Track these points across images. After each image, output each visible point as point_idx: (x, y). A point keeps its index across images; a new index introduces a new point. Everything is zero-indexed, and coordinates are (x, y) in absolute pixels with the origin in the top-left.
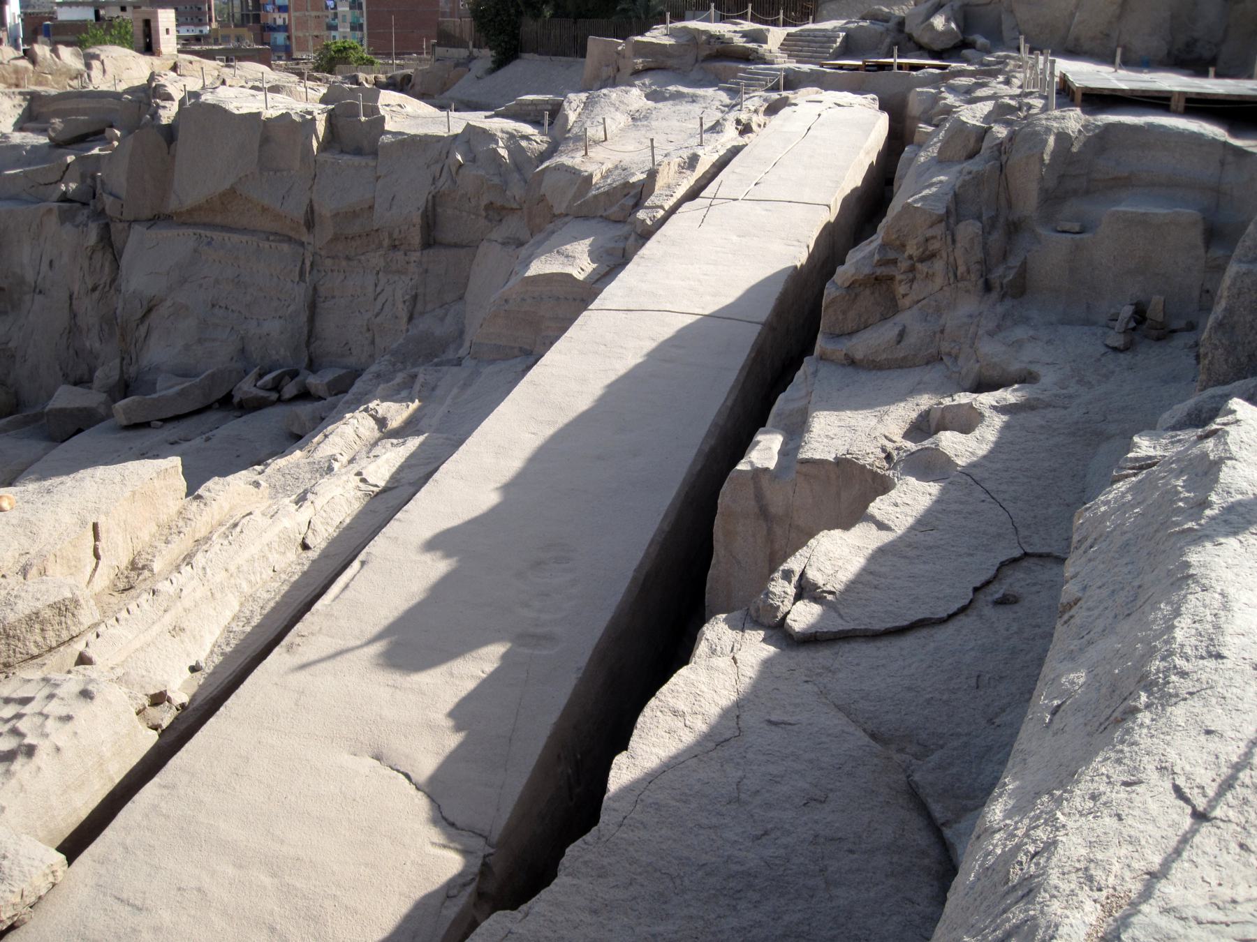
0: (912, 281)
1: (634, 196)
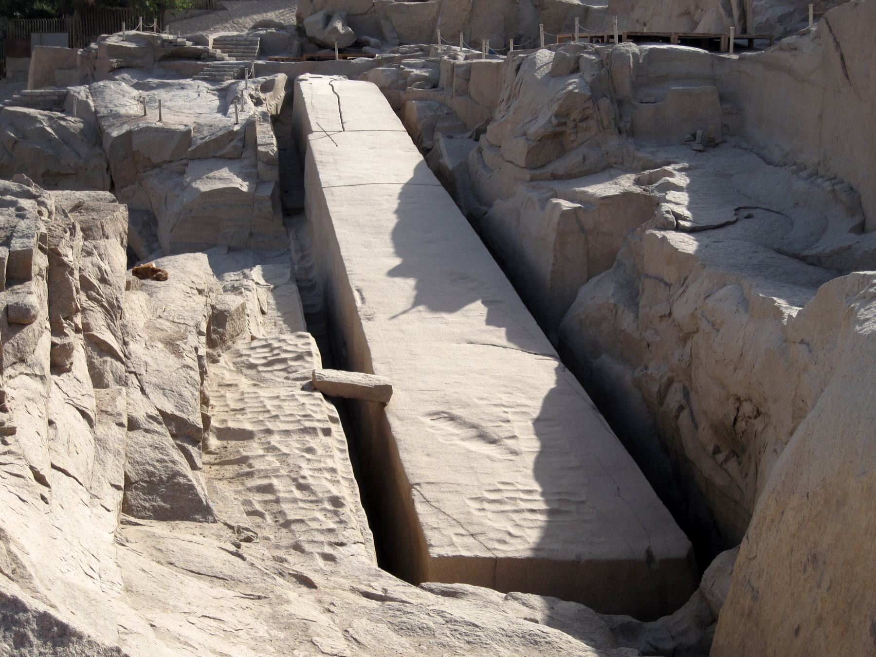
0: (577, 132)
1: (240, 140)
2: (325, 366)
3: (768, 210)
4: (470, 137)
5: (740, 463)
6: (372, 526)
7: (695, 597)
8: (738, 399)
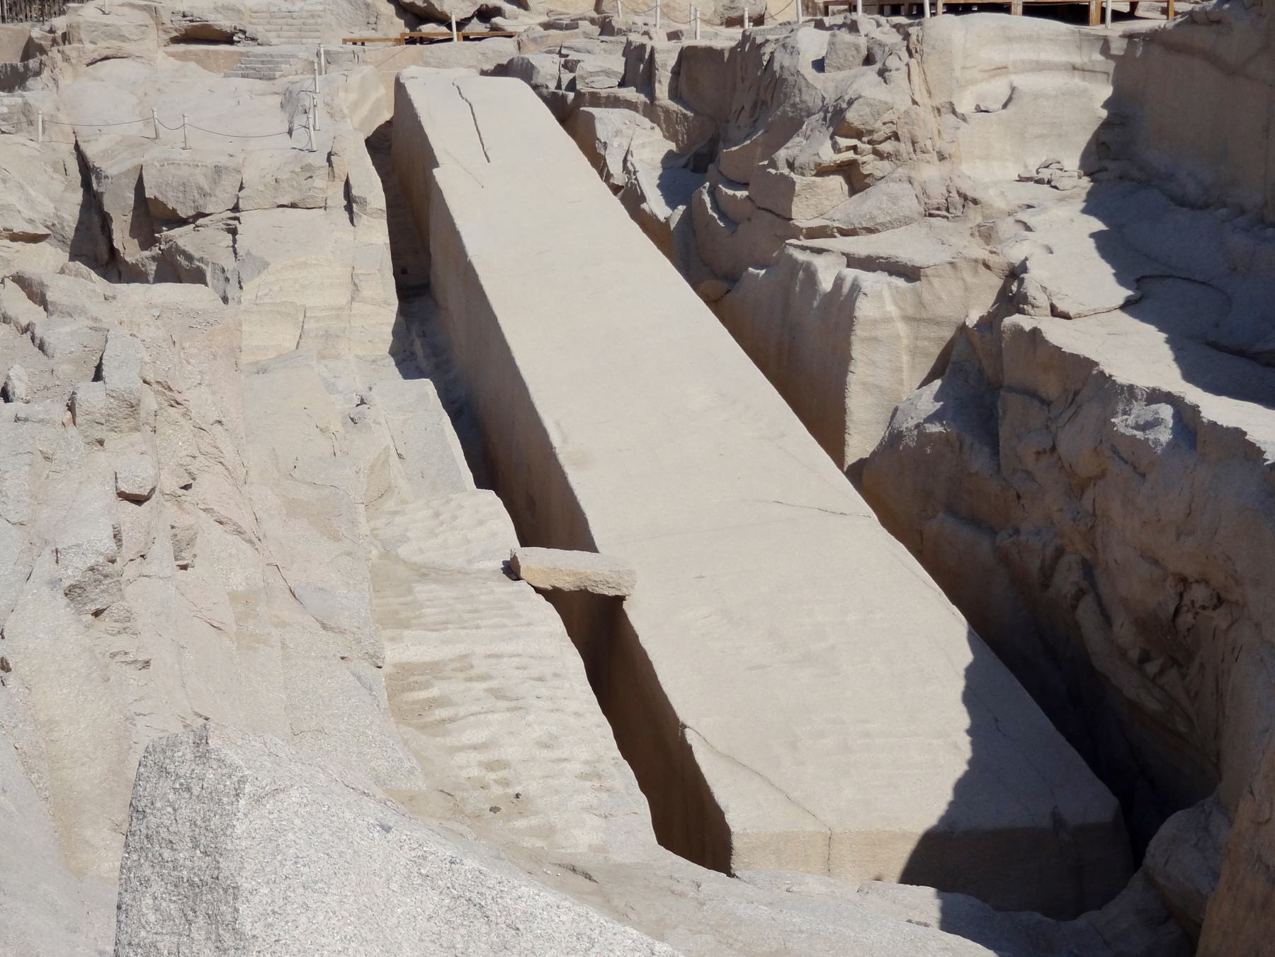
2: (525, 541)
3: (1189, 279)
4: (685, 166)
5: (1183, 676)
6: (644, 787)
7: (1137, 881)
8: (1183, 580)
